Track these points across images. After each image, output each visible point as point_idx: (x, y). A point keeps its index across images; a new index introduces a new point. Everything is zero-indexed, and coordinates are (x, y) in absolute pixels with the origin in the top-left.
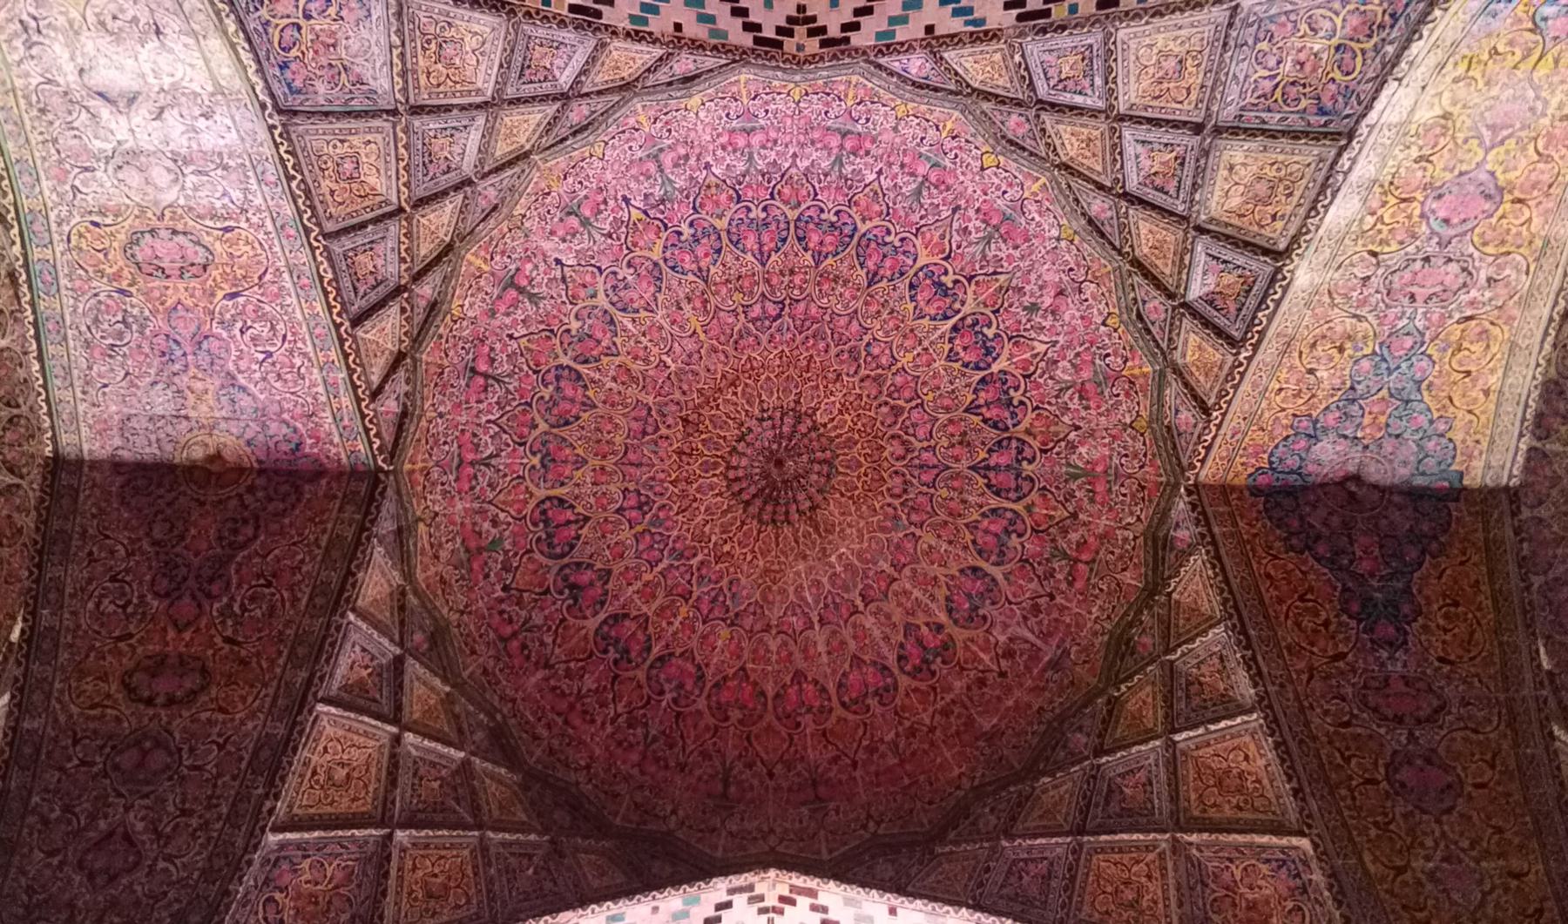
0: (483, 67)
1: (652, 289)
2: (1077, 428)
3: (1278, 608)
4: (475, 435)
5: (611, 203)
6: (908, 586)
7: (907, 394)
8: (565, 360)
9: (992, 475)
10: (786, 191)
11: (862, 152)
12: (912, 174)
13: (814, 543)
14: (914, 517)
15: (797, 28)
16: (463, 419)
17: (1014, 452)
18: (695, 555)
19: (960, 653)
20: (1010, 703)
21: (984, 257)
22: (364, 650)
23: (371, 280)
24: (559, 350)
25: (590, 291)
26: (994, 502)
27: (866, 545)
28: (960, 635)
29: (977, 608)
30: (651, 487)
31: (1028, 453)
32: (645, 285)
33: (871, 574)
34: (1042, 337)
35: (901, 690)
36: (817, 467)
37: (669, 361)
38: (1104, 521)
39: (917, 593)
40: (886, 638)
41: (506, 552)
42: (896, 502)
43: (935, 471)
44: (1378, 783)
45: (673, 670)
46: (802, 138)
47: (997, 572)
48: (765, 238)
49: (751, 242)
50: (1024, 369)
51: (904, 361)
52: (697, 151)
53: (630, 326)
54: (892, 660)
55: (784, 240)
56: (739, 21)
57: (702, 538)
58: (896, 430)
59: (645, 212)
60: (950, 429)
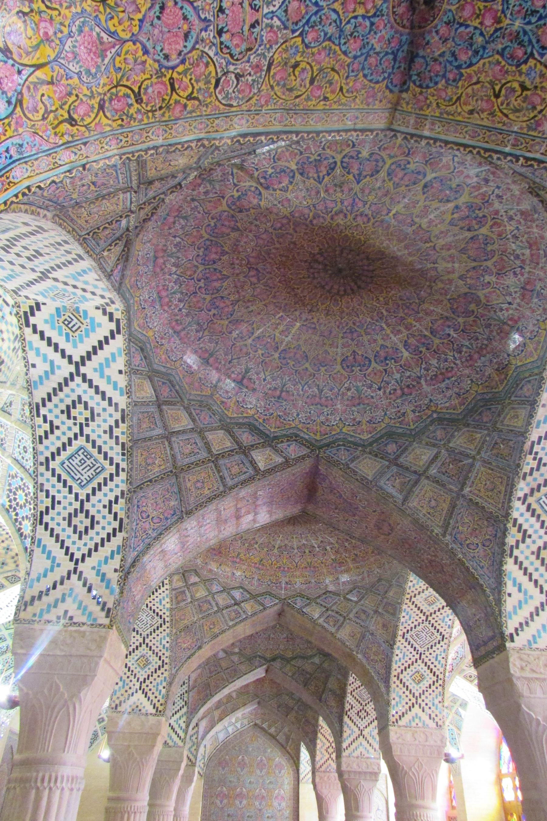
3: (497, 119)
5: (201, 345)
6: (426, 220)
8: (277, 355)
10: (189, 273)
16: (300, 402)
22: (388, 480)
23: (241, 465)
26: (383, 174)
27: (395, 238)
36: (344, 255)
41: (363, 385)
42: (372, 221)
47: (429, 177)
48: (215, 278)
49: (217, 284)
50: (296, 155)
54: (469, 235)
55: (215, 269)
60: (331, 191)
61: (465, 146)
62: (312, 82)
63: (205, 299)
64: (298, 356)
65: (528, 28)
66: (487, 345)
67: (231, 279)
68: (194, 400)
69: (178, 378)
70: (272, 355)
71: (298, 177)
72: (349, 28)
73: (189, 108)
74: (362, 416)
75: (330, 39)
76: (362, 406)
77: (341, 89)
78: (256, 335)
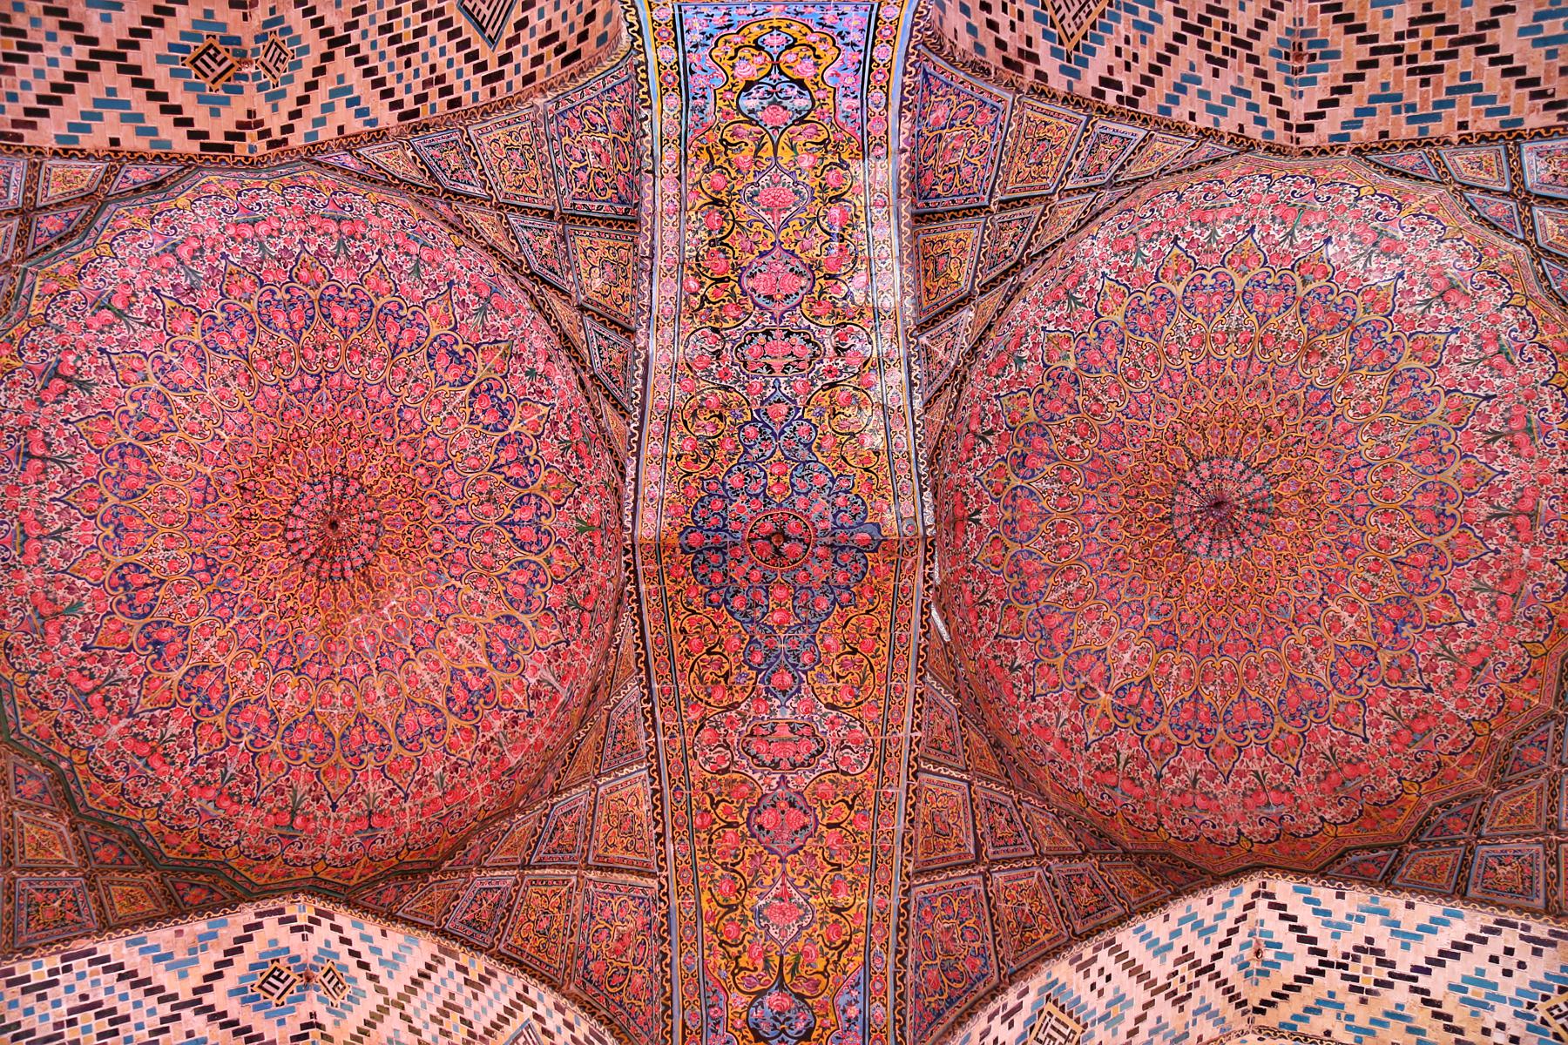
1: (198, 370)
4: (38, 513)
6: (453, 635)
7: (439, 456)
8: (127, 439)
9: (516, 529)
10: (303, 273)
12: (407, 254)
14: (454, 571)
15: (247, 132)
16: (23, 499)
19: (499, 695)
20: (532, 741)
24: (121, 432)
25: (140, 375)
31: (545, 509)
32: (190, 365)
33: (420, 623)
36: (367, 527)
37: (223, 434)
39: (461, 641)
40: (435, 682)
41: (86, 615)
42: (437, 557)
43: (469, 527)
44: (738, 825)
45: (250, 715)
47: (526, 620)
48: (294, 318)
49: (281, 320)
52: (210, 243)
53: (184, 404)
54: (440, 702)
55: (312, 318)
56: (184, 130)
57: (268, 596)
58: (432, 489)
60: (479, 487)
61: (643, 637)
63: (249, 300)
64: (134, 480)
65: (782, 657)
66: (240, 802)
67: (293, 345)
68: (23, 280)
69: (75, 249)
71: (498, 437)
72: (755, 471)
74: (17, 629)
75: (746, 451)
76: (38, 623)
77: (689, 474)
78: (172, 396)
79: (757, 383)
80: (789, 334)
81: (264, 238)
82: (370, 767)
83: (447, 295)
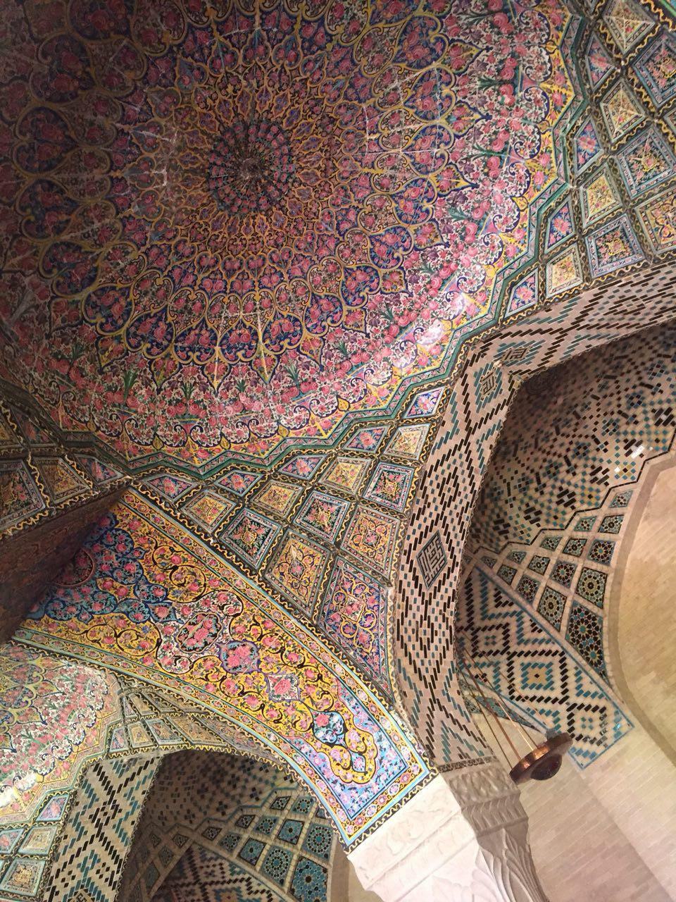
0: (652, 222)
1: (418, 160)
2: (159, 391)
5: (482, 177)
6: (107, 221)
7: (236, 285)
8: (435, 65)
9: (154, 321)
10: (397, 278)
11: (386, 333)
12: (355, 353)
13: (185, 163)
14: (155, 250)
17: (160, 341)
18: (245, 57)
19: (30, 240)
21: (286, 371)
23: (657, 59)
24: (443, 67)
25: (453, 119)
26: (135, 315)
28: (44, 245)
29: (60, 269)
30: (316, 61)
31: (155, 350)
32: (424, 157)
33: (134, 196)
34: (222, 387)
35: (22, 173)
36: (233, 196)
37: (373, 137)
38: (94, 396)
39: (97, 225)
40: (76, 182)
42: (173, 243)
43: (177, 281)
46: (417, 306)
47: (81, 297)
48: (383, 248)
49: (389, 239)
51: (257, 293)
52: (460, 246)
53: (412, 127)
54: (53, 176)
55: (373, 258)
57: (251, 72)
59: (457, 190)
60: (198, 304)
62: (175, 568)
63: (416, 231)
67: (371, 233)
70: (440, 70)
72: (131, 580)
73: (263, 620)
75: (148, 583)
77: (156, 547)
79: (189, 614)
80: (206, 644)
81: (432, 276)
82: (35, 62)
83: (318, 359)
